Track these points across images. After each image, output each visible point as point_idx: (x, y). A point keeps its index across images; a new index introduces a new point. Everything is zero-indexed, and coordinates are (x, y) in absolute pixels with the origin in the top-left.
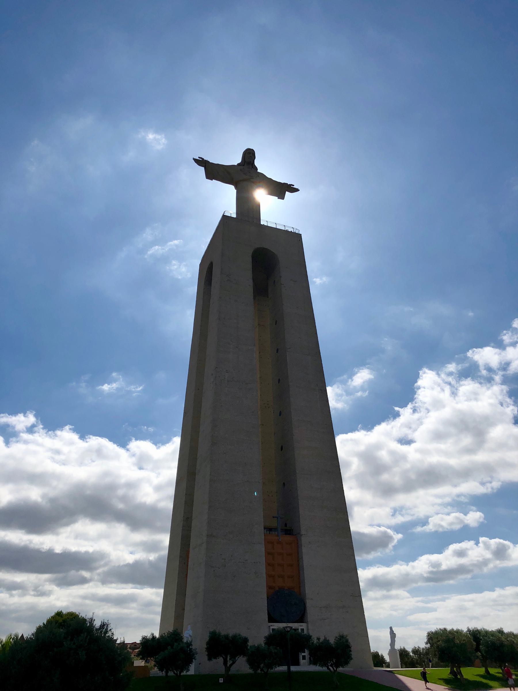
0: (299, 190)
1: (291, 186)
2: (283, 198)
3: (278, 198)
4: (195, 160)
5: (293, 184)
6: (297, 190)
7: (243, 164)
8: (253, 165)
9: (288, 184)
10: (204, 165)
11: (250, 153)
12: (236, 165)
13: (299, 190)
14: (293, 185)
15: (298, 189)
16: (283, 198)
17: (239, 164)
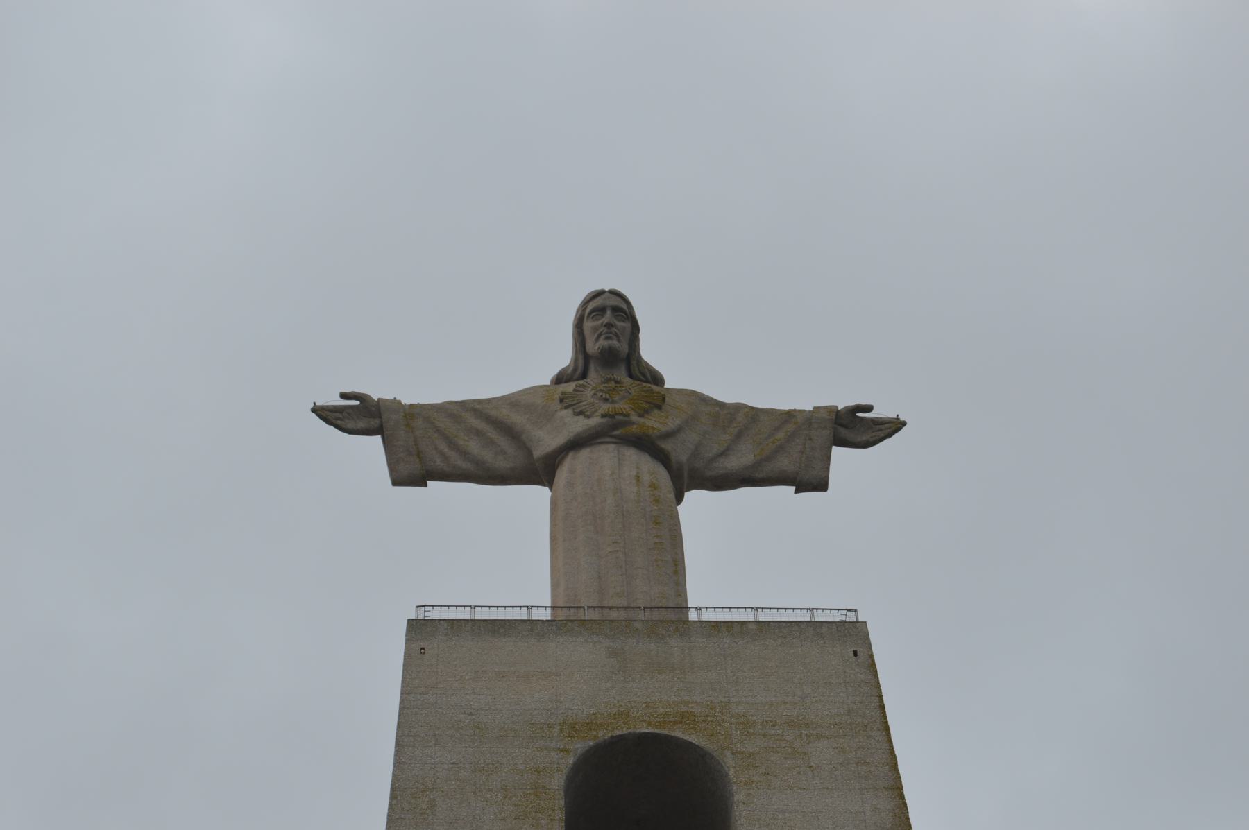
0: (904, 424)
1: (858, 414)
2: (822, 485)
3: (796, 492)
4: (326, 414)
5: (863, 402)
6: (894, 426)
7: (579, 371)
8: (634, 362)
9: (837, 407)
10: (374, 423)
11: (601, 310)
12: (548, 383)
13: (904, 424)
14: (869, 409)
15: (898, 418)
16: (822, 485)
17: (560, 379)
